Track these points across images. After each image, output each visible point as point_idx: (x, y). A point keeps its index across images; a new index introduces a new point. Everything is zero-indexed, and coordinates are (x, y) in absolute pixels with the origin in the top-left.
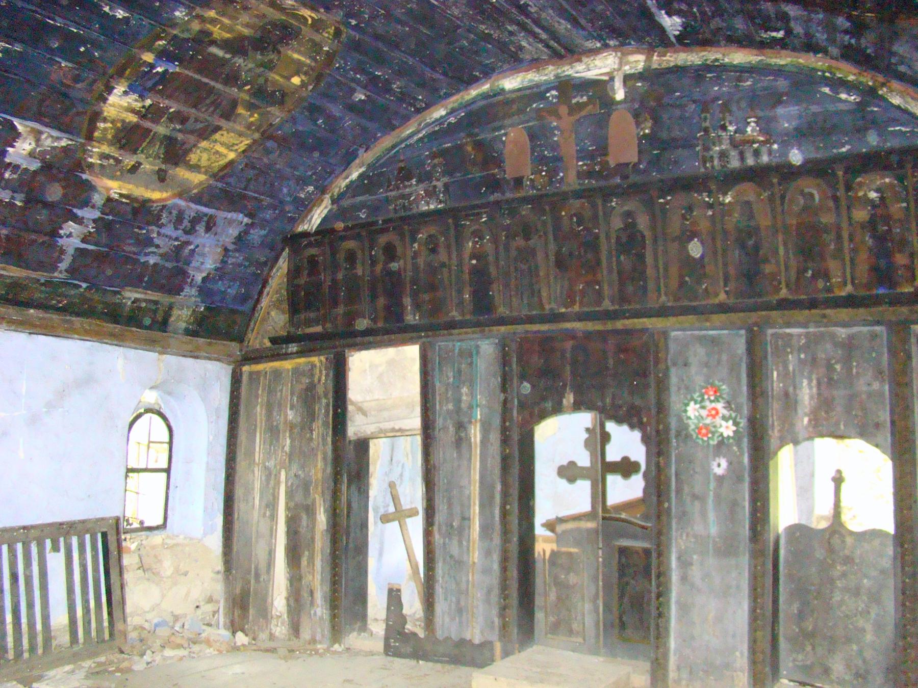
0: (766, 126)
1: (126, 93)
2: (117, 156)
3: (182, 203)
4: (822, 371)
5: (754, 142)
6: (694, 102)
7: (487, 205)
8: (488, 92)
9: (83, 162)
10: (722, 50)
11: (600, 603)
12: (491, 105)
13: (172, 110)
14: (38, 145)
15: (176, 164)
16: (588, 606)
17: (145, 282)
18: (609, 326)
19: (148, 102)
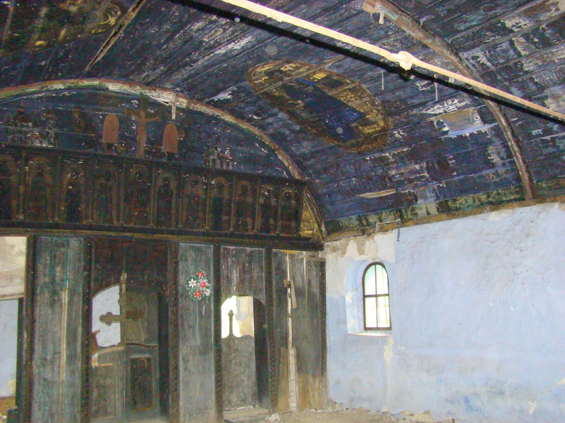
0: (233, 153)
4: (241, 266)
5: (227, 159)
6: (205, 132)
7: (88, 154)
8: (97, 86)
10: (222, 112)
11: (124, 392)
12: (96, 95)
16: (118, 395)
18: (150, 237)
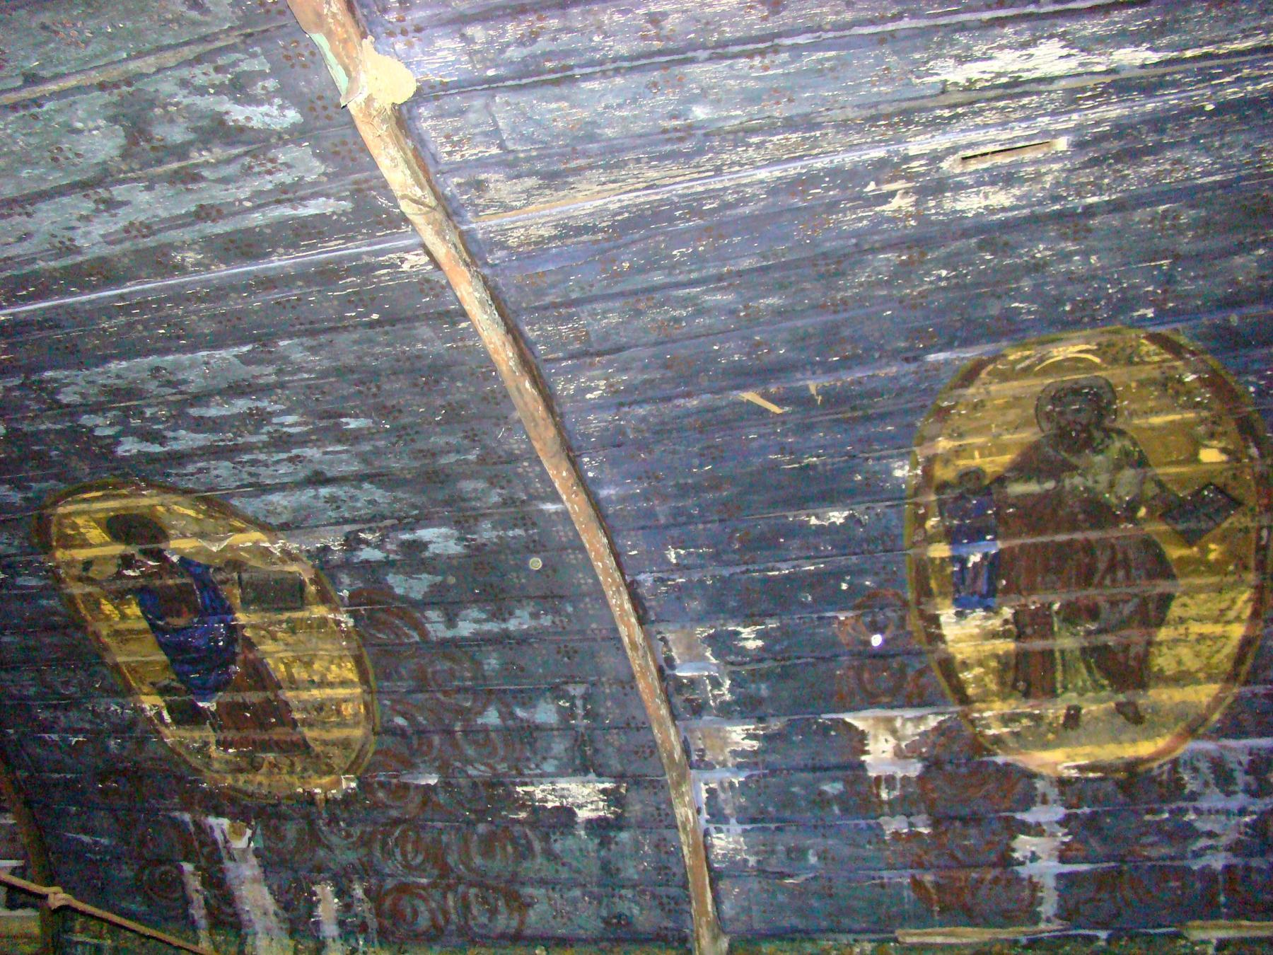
1: (960, 615)
2: (1028, 710)
3: (1209, 746)
9: (981, 739)
13: (1056, 606)
14: (899, 739)
15: (1143, 686)
17: (1226, 906)
19: (1007, 612)
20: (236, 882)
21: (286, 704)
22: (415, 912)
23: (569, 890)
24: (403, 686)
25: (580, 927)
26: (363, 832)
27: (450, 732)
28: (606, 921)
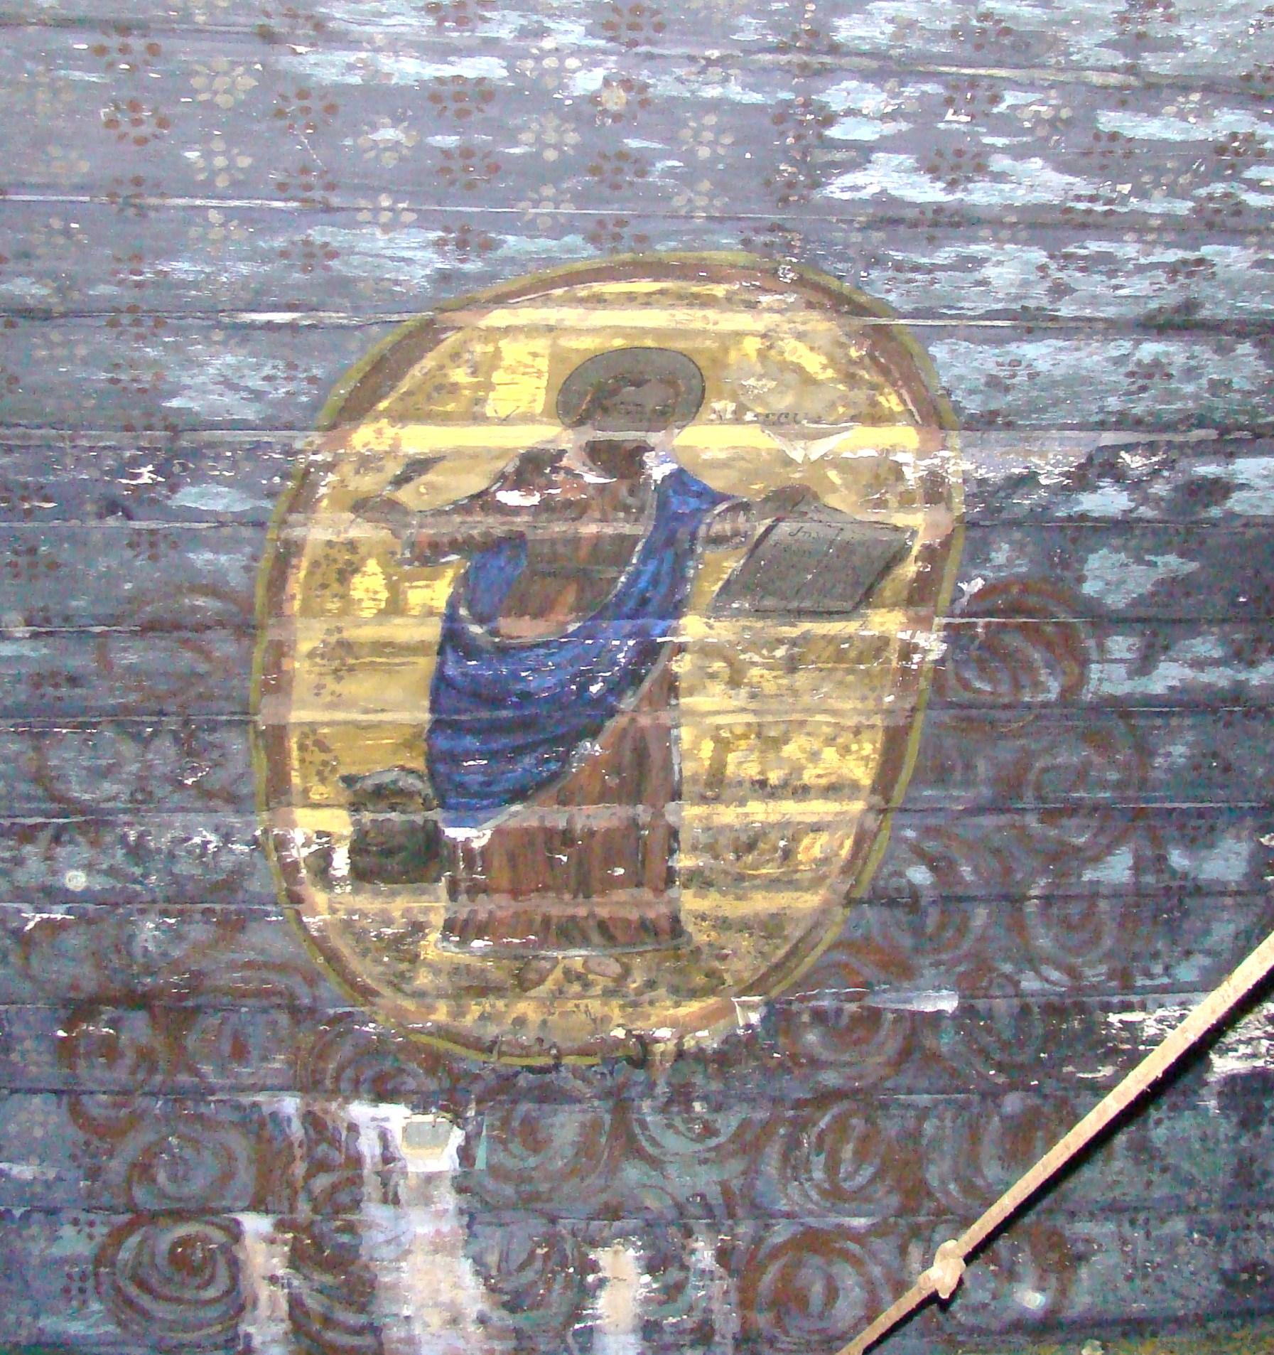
20: (387, 1252)
21: (674, 833)
22: (832, 1293)
23: (1163, 1220)
24: (958, 800)
25: (1176, 1294)
26: (745, 1125)
27: (1015, 900)
28: (1228, 1279)
